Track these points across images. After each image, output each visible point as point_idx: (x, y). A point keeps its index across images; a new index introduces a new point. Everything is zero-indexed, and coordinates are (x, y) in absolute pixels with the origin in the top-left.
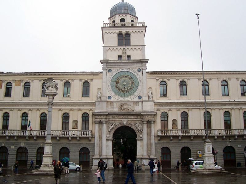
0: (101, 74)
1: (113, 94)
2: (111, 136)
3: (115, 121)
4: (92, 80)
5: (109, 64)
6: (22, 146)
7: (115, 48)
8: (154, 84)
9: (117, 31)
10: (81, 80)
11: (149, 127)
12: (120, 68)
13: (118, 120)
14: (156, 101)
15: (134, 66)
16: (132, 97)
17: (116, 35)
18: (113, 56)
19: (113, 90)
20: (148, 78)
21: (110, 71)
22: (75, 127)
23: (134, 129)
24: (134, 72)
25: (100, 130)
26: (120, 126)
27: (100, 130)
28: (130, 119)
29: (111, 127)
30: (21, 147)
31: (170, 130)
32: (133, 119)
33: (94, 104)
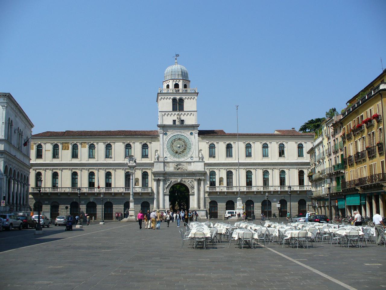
1: (169, 155)
2: (167, 191)
5: (165, 128)
6: (91, 201)
7: (170, 113)
9: (172, 97)
10: (141, 143)
11: (199, 184)
14: (206, 162)
16: (186, 158)
17: (171, 100)
18: (168, 121)
19: (169, 152)
20: (199, 141)
21: (166, 134)
23: (187, 185)
25: (158, 186)
27: (158, 186)
29: (167, 185)
30: (90, 202)
31: (218, 187)
32: (187, 177)
33: (152, 165)
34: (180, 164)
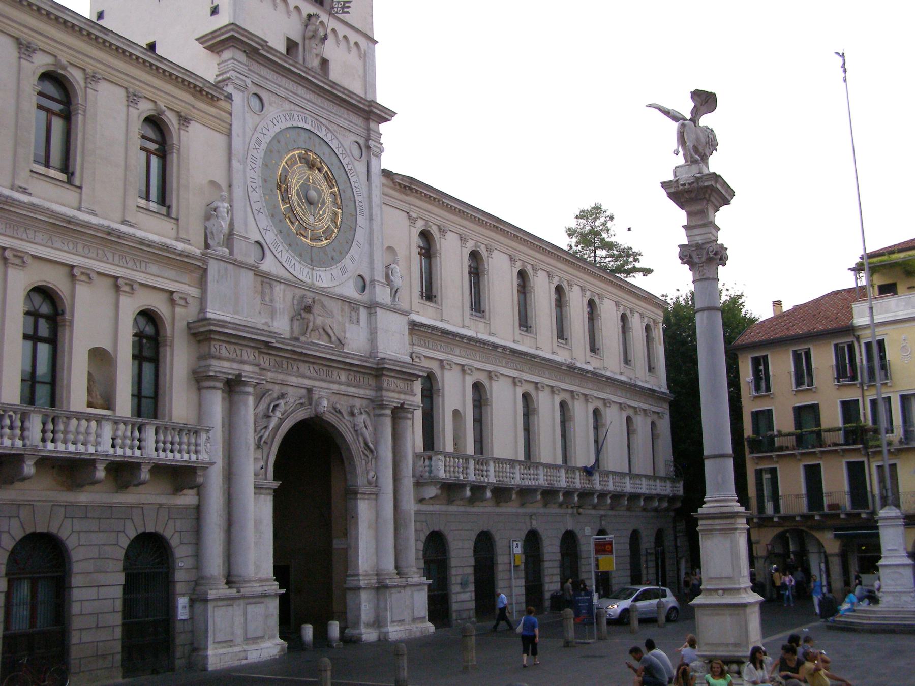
0: (223, 104)
3: (285, 389)
4: (184, 120)
5: (255, 66)
8: (398, 230)
12: (293, 106)
13: (294, 380)
15: (342, 122)
16: (335, 270)
20: (388, 200)
22: (103, 397)
23: (349, 437)
24: (341, 149)
26: (301, 415)
28: (335, 387)
32: (349, 385)
34: (323, 306)
